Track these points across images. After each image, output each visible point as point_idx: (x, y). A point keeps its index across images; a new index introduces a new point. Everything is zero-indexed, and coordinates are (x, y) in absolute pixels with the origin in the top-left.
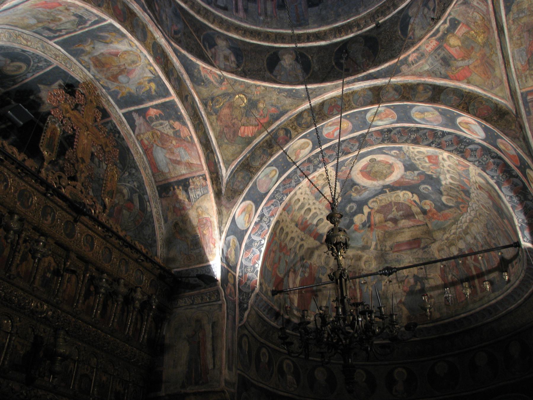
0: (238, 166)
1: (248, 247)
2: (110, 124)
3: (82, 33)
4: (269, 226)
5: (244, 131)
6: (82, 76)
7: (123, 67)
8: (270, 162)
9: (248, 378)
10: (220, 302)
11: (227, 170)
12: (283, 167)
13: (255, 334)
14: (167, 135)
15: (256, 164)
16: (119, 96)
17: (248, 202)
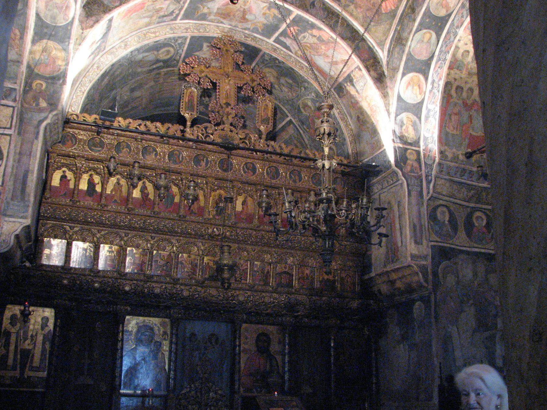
0: (393, 43)
1: (427, 118)
2: (266, 56)
3: (188, 4)
4: (438, 91)
5: (386, 7)
6: (219, 32)
7: (242, 9)
8: (415, 29)
9: (453, 246)
10: (400, 182)
11: (383, 51)
12: (436, 25)
13: (458, 202)
14: (315, 44)
15: (405, 35)
16: (260, 30)
17: (411, 75)
